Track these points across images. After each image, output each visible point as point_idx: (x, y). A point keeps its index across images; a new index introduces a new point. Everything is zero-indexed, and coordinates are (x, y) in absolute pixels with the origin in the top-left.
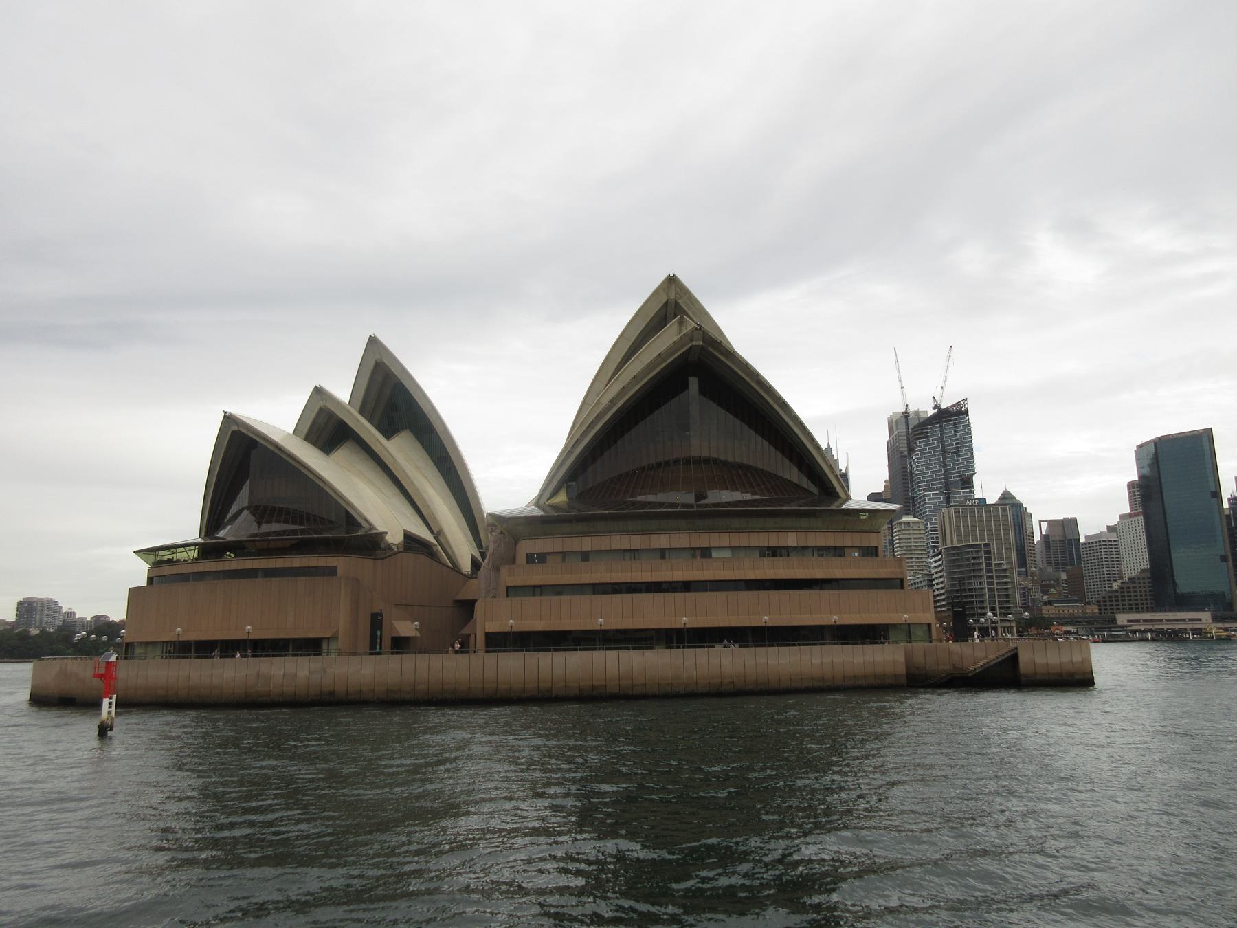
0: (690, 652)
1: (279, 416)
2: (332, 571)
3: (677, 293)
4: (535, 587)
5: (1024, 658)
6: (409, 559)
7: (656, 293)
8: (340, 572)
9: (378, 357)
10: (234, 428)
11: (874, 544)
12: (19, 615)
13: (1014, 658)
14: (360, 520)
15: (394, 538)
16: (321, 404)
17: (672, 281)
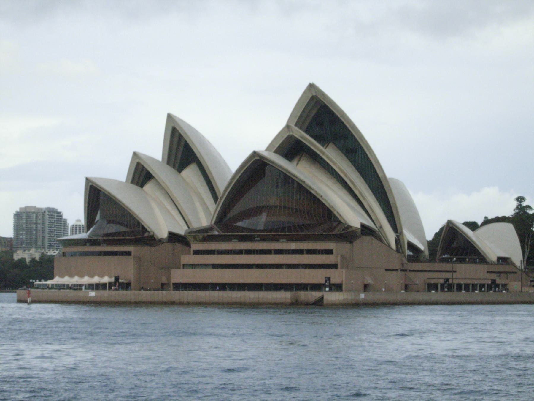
0: (186, 292)
1: (114, 172)
2: (129, 253)
3: (316, 92)
4: (192, 265)
5: (325, 298)
6: (169, 246)
7: (305, 93)
8: (132, 254)
9: (173, 125)
10: (90, 184)
11: (331, 248)
12: (17, 228)
13: (322, 299)
15: (163, 234)
16: (137, 160)
17: (311, 86)
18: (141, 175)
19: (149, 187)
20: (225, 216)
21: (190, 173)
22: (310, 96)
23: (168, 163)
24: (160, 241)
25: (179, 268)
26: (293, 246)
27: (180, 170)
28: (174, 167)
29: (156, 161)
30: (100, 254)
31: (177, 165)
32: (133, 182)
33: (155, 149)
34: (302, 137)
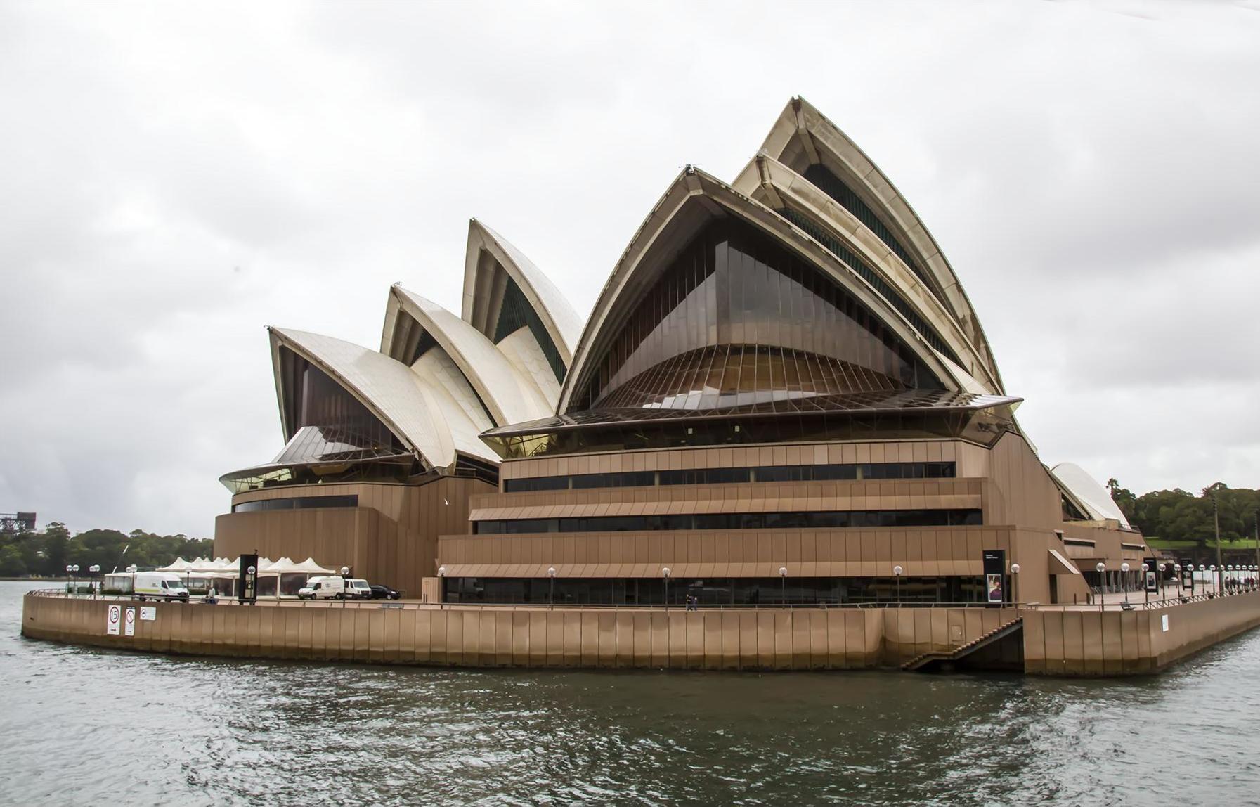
2: (352, 501)
3: (806, 120)
6: (456, 484)
14: (403, 441)
17: (797, 105)
18: (411, 339)
19: (424, 364)
20: (596, 394)
21: (519, 343)
22: (792, 131)
23: (475, 323)
24: (434, 471)
25: (465, 532)
26: (820, 454)
27: (496, 341)
28: (487, 334)
29: (446, 314)
30: (288, 503)
31: (494, 332)
32: (393, 355)
33: (444, 293)
34: (794, 190)
